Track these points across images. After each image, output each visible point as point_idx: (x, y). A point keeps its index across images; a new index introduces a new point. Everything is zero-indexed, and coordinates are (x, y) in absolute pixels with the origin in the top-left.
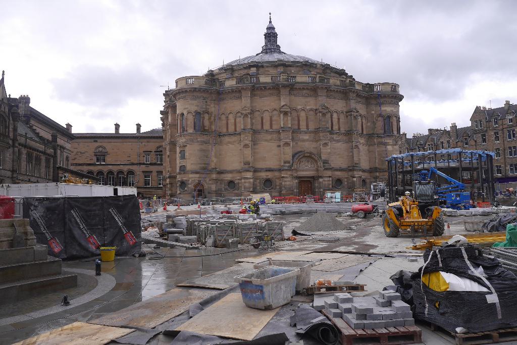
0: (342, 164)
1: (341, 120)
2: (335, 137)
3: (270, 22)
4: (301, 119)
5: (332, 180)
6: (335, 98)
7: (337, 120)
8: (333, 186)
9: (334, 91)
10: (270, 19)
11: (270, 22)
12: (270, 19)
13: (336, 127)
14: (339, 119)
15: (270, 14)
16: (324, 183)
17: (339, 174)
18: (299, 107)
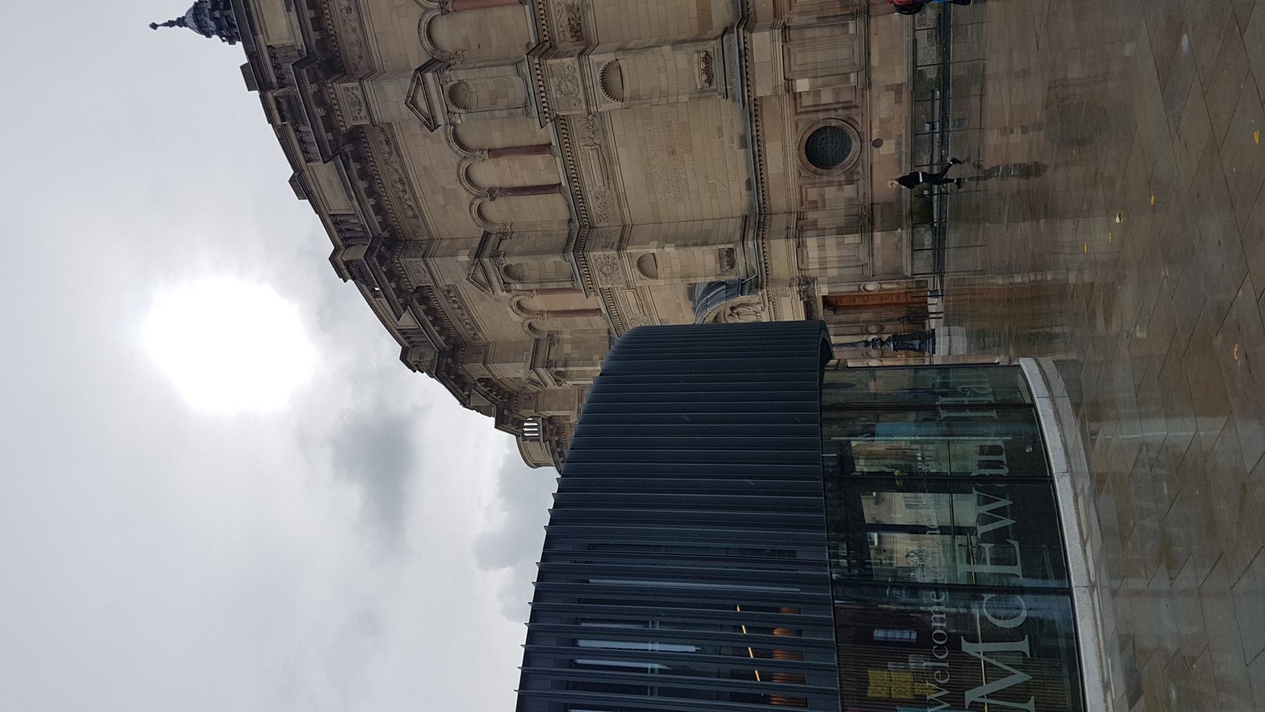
0: (720, 130)
1: (498, 141)
2: (593, 182)
3: (181, 22)
4: (560, 307)
5: (813, 185)
6: (405, 181)
7: (504, 161)
8: (850, 182)
9: (379, 209)
10: (170, 24)
11: (181, 22)
12: (170, 24)
13: (543, 170)
14: (494, 153)
15: (154, 26)
16: (833, 272)
17: (782, 156)
18: (516, 318)
